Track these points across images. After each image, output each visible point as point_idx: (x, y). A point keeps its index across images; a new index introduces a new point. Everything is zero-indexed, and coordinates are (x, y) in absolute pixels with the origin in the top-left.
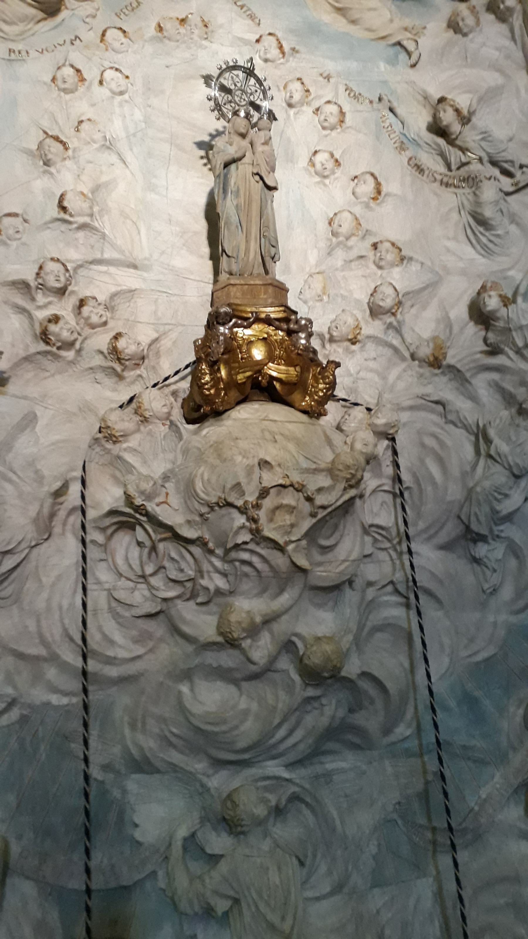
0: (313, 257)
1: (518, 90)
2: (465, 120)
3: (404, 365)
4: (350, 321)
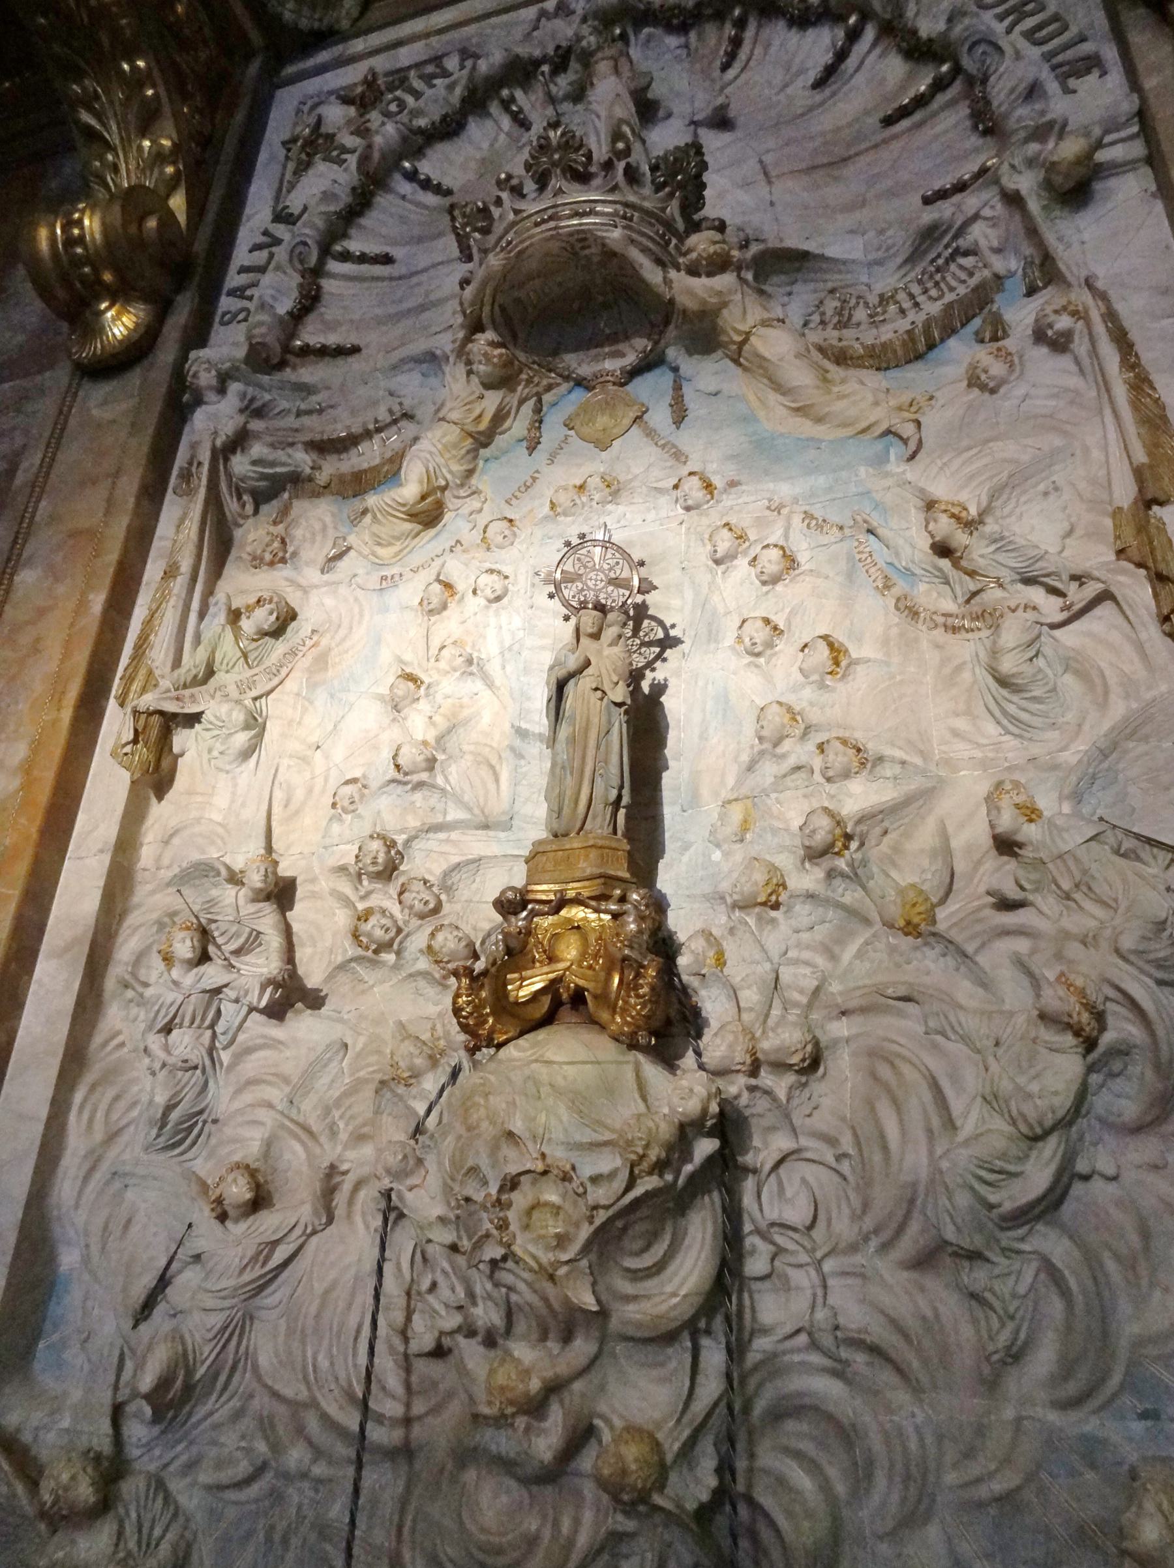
0: (731, 781)
1: (1086, 450)
2: (970, 525)
3: (865, 934)
4: (760, 877)
